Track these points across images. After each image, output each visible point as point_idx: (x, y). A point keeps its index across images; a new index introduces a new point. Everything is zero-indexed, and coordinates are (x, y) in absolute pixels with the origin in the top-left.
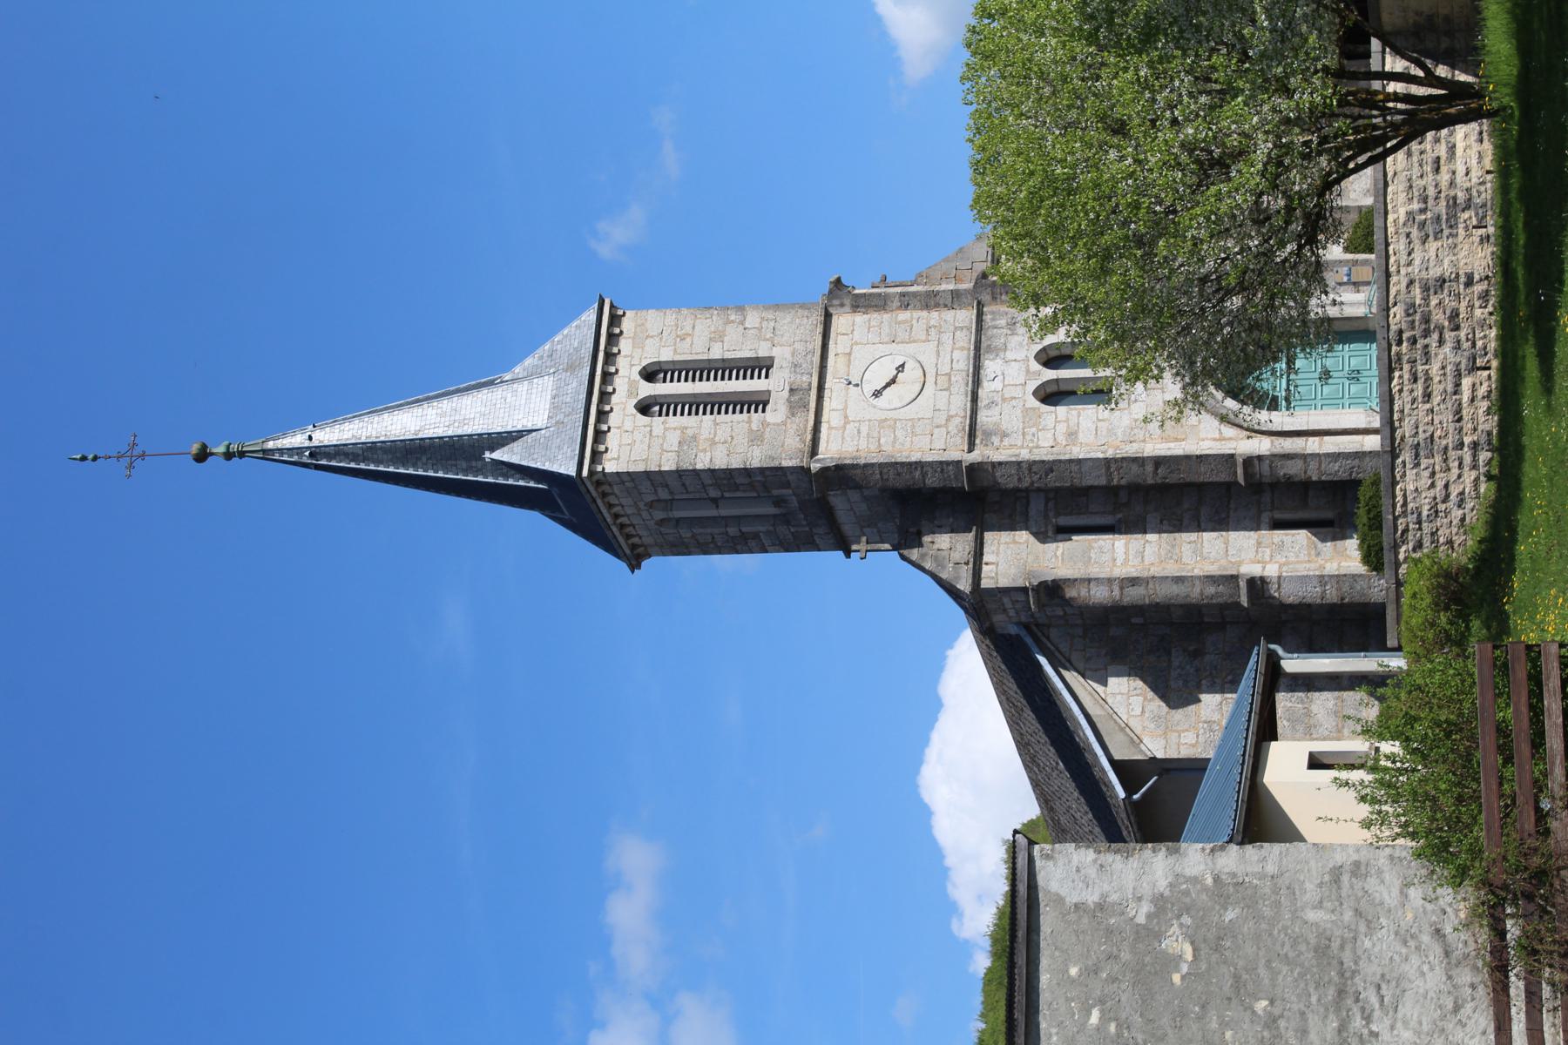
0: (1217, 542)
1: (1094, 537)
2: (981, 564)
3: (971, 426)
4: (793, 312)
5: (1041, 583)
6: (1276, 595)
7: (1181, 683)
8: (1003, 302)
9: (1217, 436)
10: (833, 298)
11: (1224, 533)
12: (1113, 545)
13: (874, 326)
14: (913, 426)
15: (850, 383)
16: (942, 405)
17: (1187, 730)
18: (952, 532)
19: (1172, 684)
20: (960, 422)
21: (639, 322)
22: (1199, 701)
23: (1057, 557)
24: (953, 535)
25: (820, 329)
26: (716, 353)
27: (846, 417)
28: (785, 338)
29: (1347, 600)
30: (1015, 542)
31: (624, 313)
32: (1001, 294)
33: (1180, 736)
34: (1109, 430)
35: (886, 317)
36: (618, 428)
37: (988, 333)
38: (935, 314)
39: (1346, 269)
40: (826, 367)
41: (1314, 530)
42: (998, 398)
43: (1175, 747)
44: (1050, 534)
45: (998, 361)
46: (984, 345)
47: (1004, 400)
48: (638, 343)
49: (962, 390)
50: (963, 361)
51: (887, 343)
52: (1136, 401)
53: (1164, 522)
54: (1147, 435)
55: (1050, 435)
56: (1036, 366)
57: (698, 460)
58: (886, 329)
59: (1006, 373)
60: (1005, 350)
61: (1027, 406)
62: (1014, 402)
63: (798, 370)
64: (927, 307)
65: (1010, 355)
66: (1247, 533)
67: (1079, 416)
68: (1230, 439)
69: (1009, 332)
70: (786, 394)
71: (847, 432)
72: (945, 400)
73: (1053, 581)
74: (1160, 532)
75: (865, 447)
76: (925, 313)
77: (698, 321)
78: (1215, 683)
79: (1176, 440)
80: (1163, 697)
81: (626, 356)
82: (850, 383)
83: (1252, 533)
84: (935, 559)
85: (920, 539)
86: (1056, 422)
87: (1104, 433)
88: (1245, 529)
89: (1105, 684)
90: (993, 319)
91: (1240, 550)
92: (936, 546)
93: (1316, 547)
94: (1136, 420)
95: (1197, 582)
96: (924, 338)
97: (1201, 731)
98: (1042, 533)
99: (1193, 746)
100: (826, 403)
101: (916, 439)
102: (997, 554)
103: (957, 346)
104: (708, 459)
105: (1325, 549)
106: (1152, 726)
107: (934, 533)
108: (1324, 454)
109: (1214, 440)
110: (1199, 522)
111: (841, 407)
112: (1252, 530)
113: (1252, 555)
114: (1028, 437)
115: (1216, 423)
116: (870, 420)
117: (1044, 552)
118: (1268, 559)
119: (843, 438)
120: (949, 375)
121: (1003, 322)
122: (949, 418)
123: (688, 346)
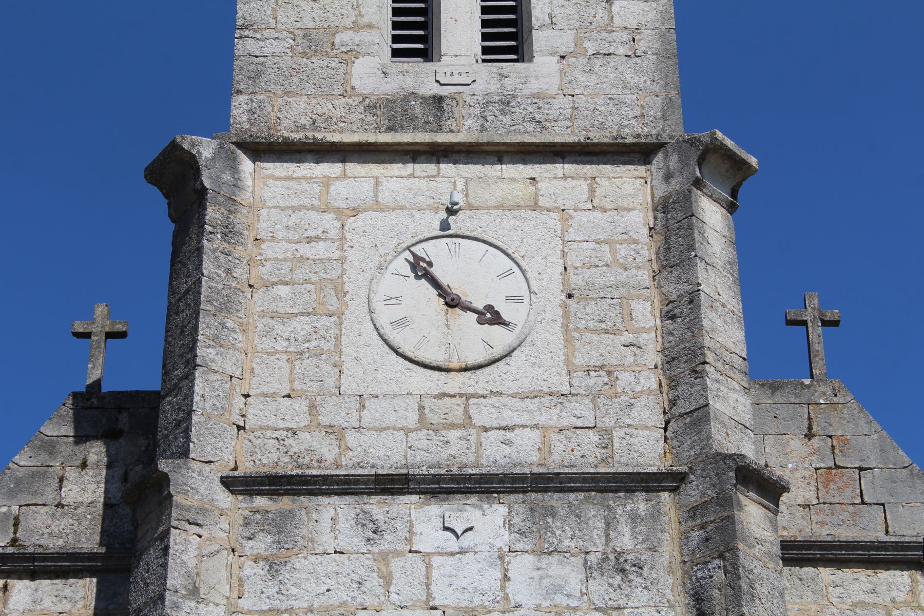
4: (656, 87)
8: (685, 536)
13: (613, 252)
14: (318, 353)
15: (451, 212)
16: (373, 413)
18: (107, 505)
24: (100, 505)
25: (597, 137)
27: (355, 212)
28: (582, 78)
32: (703, 527)
35: (644, 276)
38: (650, 381)
40: (501, 161)
42: (386, 543)
45: (504, 539)
46: (554, 500)
47: (384, 557)
49: (421, 457)
58: (603, 278)
59: (469, 557)
62: (374, 581)
63: (495, 108)
64: (670, 360)
69: (593, 559)
70: (430, 89)
71: (314, 215)
72: (391, 419)
75: (270, 254)
76: (652, 356)
84: (38, 475)
85: (96, 438)
90: (634, 518)
92: (71, 473)
96: (580, 360)
100: (396, 169)
103: (555, 437)
107: (109, 466)
111: (385, 197)
116: (342, 260)
119: (294, 209)
121: (625, 540)
122: (334, 432)
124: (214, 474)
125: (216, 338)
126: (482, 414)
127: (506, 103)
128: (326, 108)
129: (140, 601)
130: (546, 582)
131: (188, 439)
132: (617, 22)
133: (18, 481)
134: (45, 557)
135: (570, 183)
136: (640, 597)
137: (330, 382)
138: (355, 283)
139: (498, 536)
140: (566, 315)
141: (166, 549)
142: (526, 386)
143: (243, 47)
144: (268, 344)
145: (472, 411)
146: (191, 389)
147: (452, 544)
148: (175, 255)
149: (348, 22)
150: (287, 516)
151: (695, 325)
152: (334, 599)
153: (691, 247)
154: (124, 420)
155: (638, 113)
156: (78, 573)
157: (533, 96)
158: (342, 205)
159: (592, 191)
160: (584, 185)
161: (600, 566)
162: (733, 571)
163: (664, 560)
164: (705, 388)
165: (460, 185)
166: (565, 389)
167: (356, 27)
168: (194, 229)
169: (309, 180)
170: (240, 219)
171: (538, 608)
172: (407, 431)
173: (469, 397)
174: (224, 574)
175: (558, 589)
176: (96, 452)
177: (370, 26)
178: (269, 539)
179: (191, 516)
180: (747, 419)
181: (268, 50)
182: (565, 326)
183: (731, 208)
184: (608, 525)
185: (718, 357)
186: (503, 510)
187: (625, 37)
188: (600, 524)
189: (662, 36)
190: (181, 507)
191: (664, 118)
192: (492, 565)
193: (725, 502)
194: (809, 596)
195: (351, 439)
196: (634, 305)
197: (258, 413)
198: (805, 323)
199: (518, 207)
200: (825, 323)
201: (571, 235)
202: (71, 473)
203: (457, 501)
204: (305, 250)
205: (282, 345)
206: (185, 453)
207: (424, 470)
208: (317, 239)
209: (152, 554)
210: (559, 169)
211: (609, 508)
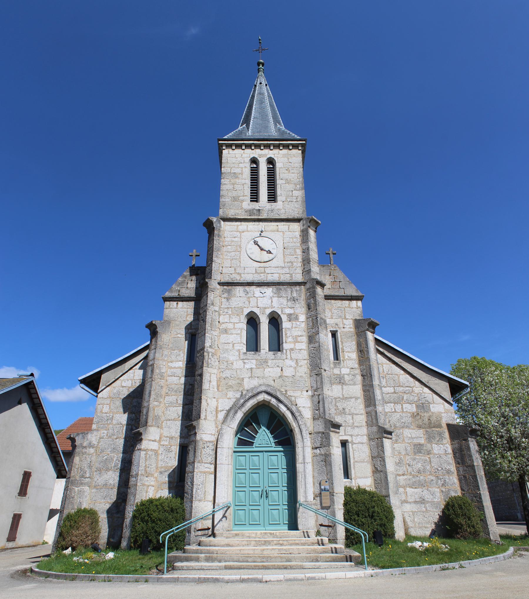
0: (176, 415)
1: (186, 351)
2: (178, 301)
3: (233, 283)
5: (155, 325)
6: (136, 448)
7: (135, 404)
8: (306, 294)
9: (219, 409)
10: (306, 220)
11: (180, 418)
12: (180, 361)
14: (236, 259)
15: (262, 232)
17: (110, 408)
19: (135, 400)
20: (237, 278)
21: (296, 155)
22: (124, 413)
23: (177, 334)
25: (290, 217)
26: (279, 182)
27: (243, 232)
29: (129, 491)
30: (187, 315)
31: (300, 150)
32: (309, 292)
33: (108, 404)
34: (227, 350)
35: (299, 245)
36: (244, 153)
37: (289, 290)
38: (300, 264)
39: (328, 488)
40: (271, 222)
41: (176, 470)
43: (103, 402)
44: (190, 331)
45: (272, 294)
46: (281, 287)
47: (249, 298)
48: (284, 156)
50: (270, 278)
51: (283, 245)
52: (244, 363)
53: (191, 386)
54: (222, 370)
55: (226, 320)
56: (268, 311)
57: (225, 180)
58: (291, 245)
59: (265, 298)
60: (278, 297)
61: (244, 308)
62: (247, 302)
65: (275, 300)
66: (179, 431)
67: (237, 334)
68: (217, 417)
69: (289, 298)
70: (258, 208)
71: (235, 233)
72: (250, 272)
73: (157, 332)
74: (185, 384)
75: (227, 240)
76: (300, 260)
77: (296, 174)
78: (133, 420)
79: (218, 386)
80: (129, 396)
81: (279, 152)
82: (262, 232)
83: (179, 434)
84: (183, 282)
85: (194, 275)
86: (234, 323)
87: (225, 347)
88: (182, 430)
89: (140, 368)
90: (296, 291)
91: (169, 427)
92: (189, 282)
93: (165, 471)
94: (232, 364)
95: (148, 404)
96: (286, 261)
97: (108, 415)
98: (191, 327)
99: (101, 411)
100: (251, 223)
101: (229, 261)
102: (182, 308)
104: (226, 183)
105: (164, 477)
106: (115, 391)
107: (196, 281)
108: (194, 475)
109: (217, 408)
110: (188, 404)
111: (249, 229)
112: (181, 433)
113: (166, 433)
114: (226, 310)
115: (228, 408)
116: (241, 241)
117: (180, 329)
118: (161, 444)
120: (265, 272)
121: (295, 295)
122: (238, 274)
123: (283, 172)
124: (216, 282)
125: (216, 256)
126: (268, 271)
127: (272, 211)
128: (237, 211)
129: (203, 306)
130: (280, 303)
131: (211, 275)
132: (294, 195)
133: (179, 283)
134: (185, 298)
135: (285, 226)
136: (297, 305)
137: (238, 265)
138: (243, 246)
139: (270, 294)
140: (284, 252)
141: (207, 296)
142: (276, 265)
143: (221, 200)
144: (226, 257)
145: (266, 270)
146: (212, 266)
147: (262, 295)
148: (208, 240)
149: (242, 195)
150: (230, 290)
151: (308, 254)
152: (239, 306)
153: (308, 239)
154: (199, 272)
155: (298, 212)
156: (191, 301)
157: (277, 209)
158: (240, 230)
159: (289, 228)
160: (287, 227)
161: (290, 300)
162: (315, 301)
163: (302, 299)
164: (310, 266)
165: (263, 227)
166: (283, 266)
167: (243, 196)
168: (212, 235)
169: (234, 225)
170: (221, 233)
171: (278, 307)
172: (253, 274)
173: (265, 267)
174: (218, 301)
175: (282, 304)
176: (194, 278)
177: (246, 196)
178: (227, 294)
179: (212, 290)
180: (318, 272)
181: (226, 201)
182: (283, 254)
183: (315, 231)
184: (291, 292)
185: (313, 260)
186: (271, 289)
187: (295, 198)
188: (290, 292)
189: (302, 198)
190: (210, 288)
191: (303, 213)
192: (269, 299)
193: (314, 288)
194: (330, 306)
195: (242, 275)
196: (297, 250)
197: (225, 271)
198: (329, 254)
199: (275, 231)
200: (333, 254)
201: (285, 237)
202: (189, 282)
203: (263, 287)
204: (234, 239)
205: (229, 257)
206: (211, 278)
207: (256, 281)
208: (236, 237)
209: (205, 297)
210: (282, 223)
211: (292, 289)
